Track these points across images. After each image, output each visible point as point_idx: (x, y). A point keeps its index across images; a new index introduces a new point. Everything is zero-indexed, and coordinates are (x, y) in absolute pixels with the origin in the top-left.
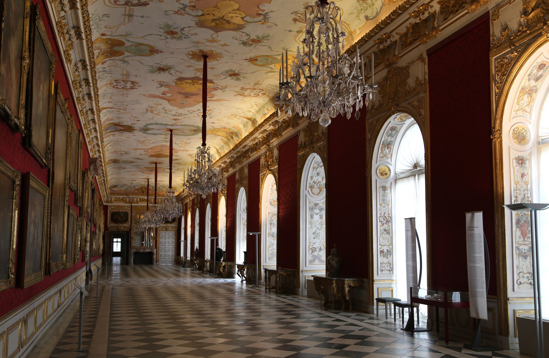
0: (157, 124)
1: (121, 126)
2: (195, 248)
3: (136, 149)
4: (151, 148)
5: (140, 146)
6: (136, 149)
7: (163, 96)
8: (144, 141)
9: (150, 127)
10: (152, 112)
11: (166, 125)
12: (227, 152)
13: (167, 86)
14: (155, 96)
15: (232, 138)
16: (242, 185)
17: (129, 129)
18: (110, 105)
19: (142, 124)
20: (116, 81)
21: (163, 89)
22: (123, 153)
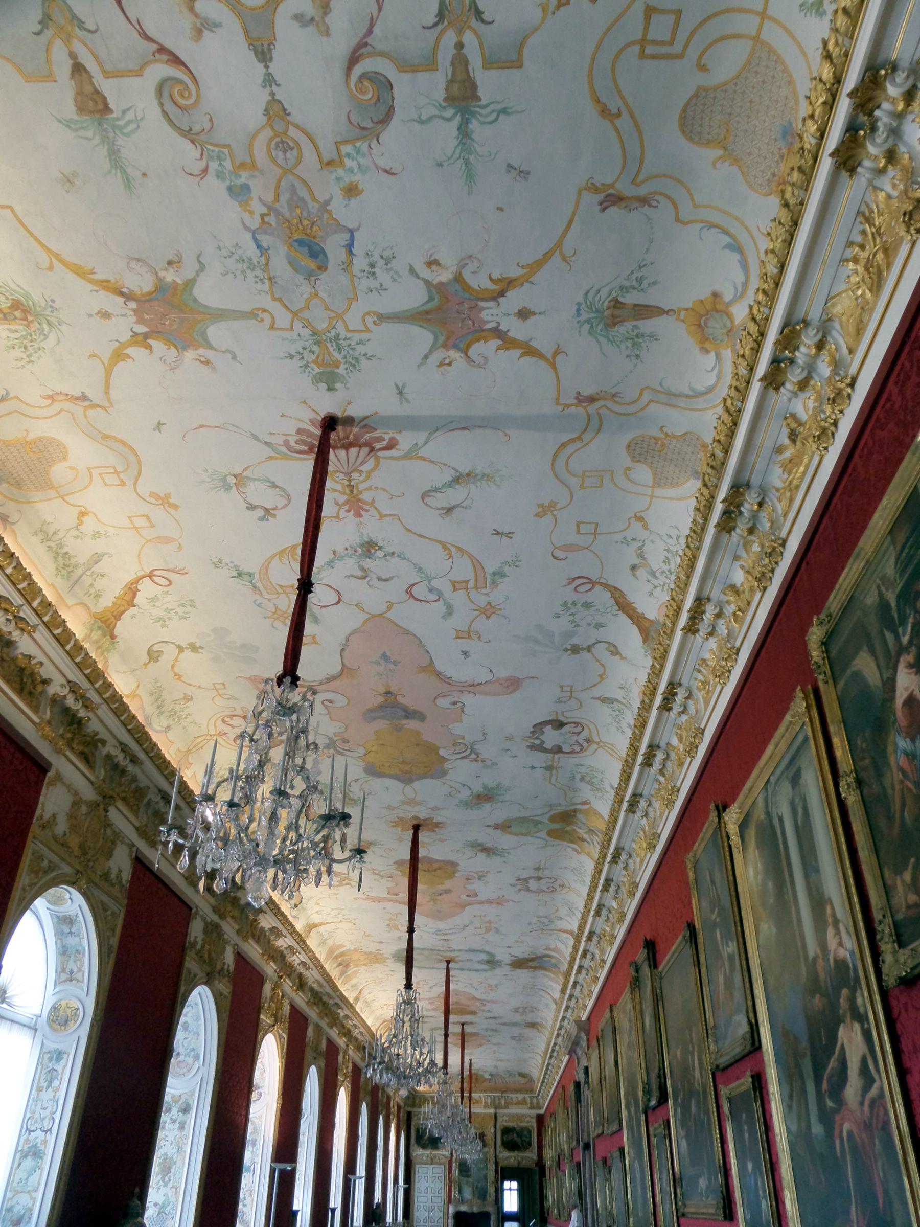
0: (477, 970)
1: (532, 968)
2: (376, 1201)
3: (500, 902)
4: (463, 906)
5: (490, 911)
6: (500, 902)
7: (483, 1003)
8: (488, 930)
9: (486, 967)
10: (490, 986)
11: (462, 970)
12: (369, 1023)
13: (484, 1011)
14: (492, 1002)
15: (340, 965)
16: (315, 1061)
17: (519, 964)
18: (542, 993)
19: (498, 971)
20: (532, 1011)
21: (486, 1008)
22: (533, 884)
